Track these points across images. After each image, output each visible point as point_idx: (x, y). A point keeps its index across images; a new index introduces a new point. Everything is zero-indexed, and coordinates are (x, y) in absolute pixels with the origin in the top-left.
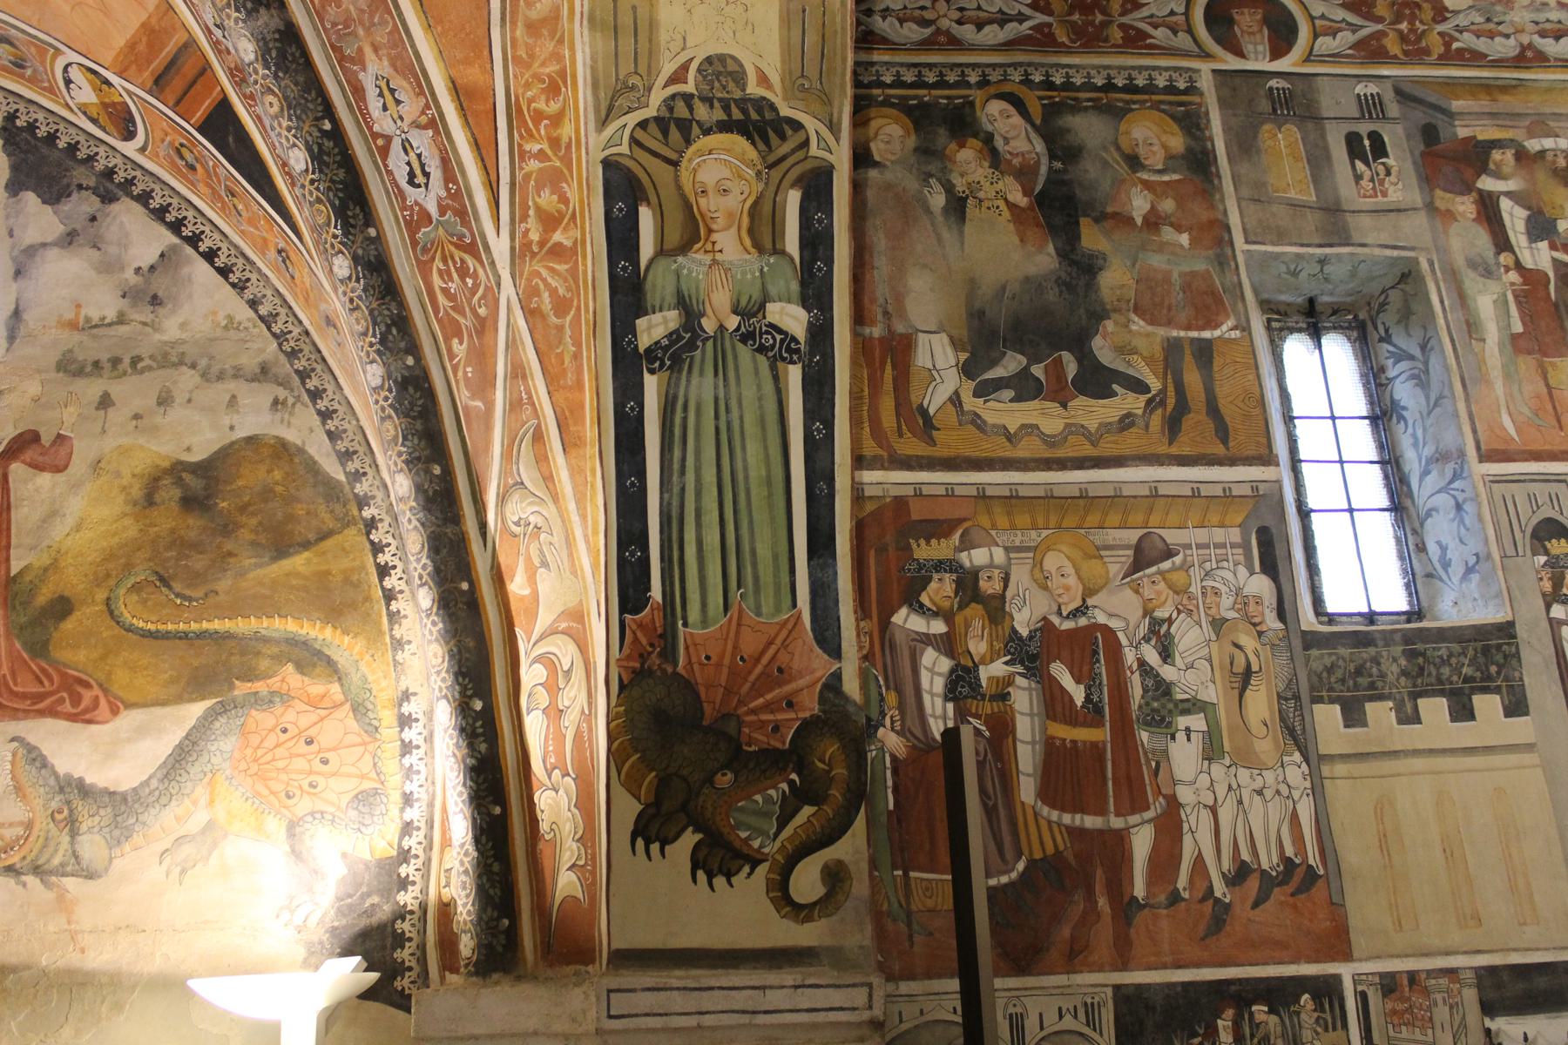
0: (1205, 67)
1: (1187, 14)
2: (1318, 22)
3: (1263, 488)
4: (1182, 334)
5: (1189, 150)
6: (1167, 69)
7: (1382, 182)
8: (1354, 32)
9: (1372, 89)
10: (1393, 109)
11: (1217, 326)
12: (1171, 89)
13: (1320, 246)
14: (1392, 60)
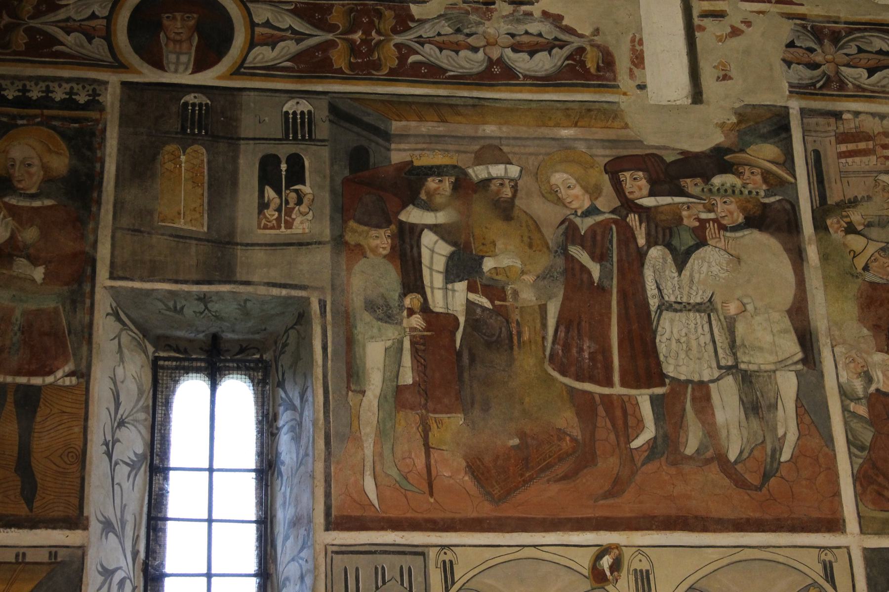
0: (114, 79)
1: (109, 18)
2: (258, 30)
3: (62, 555)
4: (9, 379)
5: (73, 171)
6: (69, 80)
7: (289, 212)
8: (298, 42)
9: (305, 106)
10: (323, 130)
11: (51, 372)
12: (69, 103)
13: (198, 283)
14: (340, 76)
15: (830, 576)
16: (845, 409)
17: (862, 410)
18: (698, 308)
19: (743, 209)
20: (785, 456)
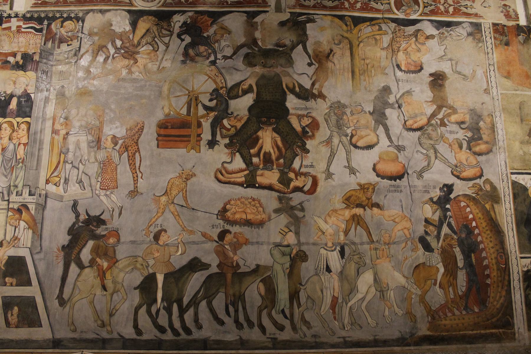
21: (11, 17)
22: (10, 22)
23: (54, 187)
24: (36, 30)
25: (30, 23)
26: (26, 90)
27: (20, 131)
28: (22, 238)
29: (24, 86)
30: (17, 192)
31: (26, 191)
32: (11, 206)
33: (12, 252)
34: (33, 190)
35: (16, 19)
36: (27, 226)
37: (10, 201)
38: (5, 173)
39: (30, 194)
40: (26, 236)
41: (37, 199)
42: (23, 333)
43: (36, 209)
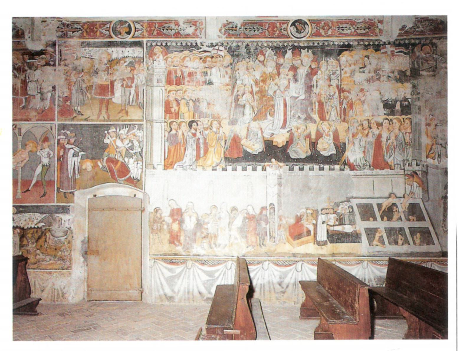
15: (52, 129)
16: (58, 99)
17: (61, 99)
18: (35, 81)
19: (46, 62)
20: (47, 108)
21: (386, 45)
22: (386, 48)
23: (432, 160)
24: (405, 54)
25: (400, 48)
26: (405, 97)
27: (405, 124)
28: (416, 193)
29: (403, 94)
30: (409, 164)
31: (414, 163)
32: (406, 173)
33: (411, 201)
34: (418, 162)
35: (389, 46)
36: (418, 185)
37: (405, 169)
38: (400, 152)
39: (417, 165)
40: (418, 191)
41: (422, 168)
42: (425, 248)
43: (422, 174)
